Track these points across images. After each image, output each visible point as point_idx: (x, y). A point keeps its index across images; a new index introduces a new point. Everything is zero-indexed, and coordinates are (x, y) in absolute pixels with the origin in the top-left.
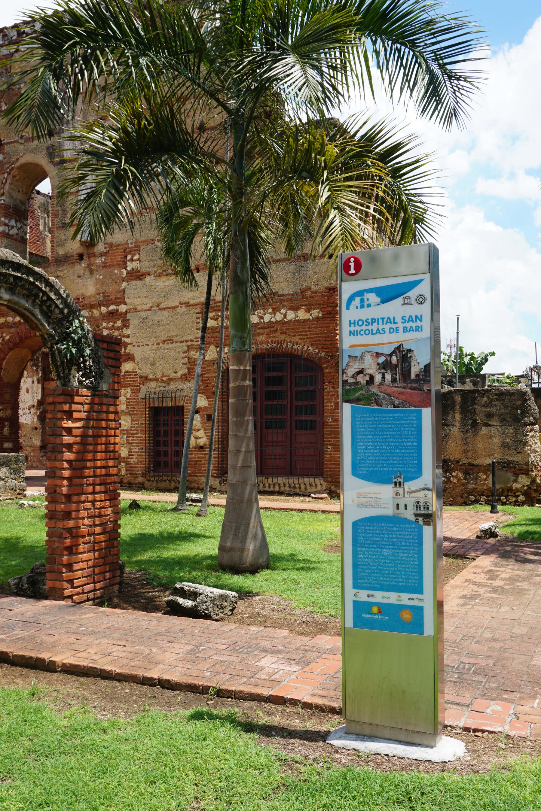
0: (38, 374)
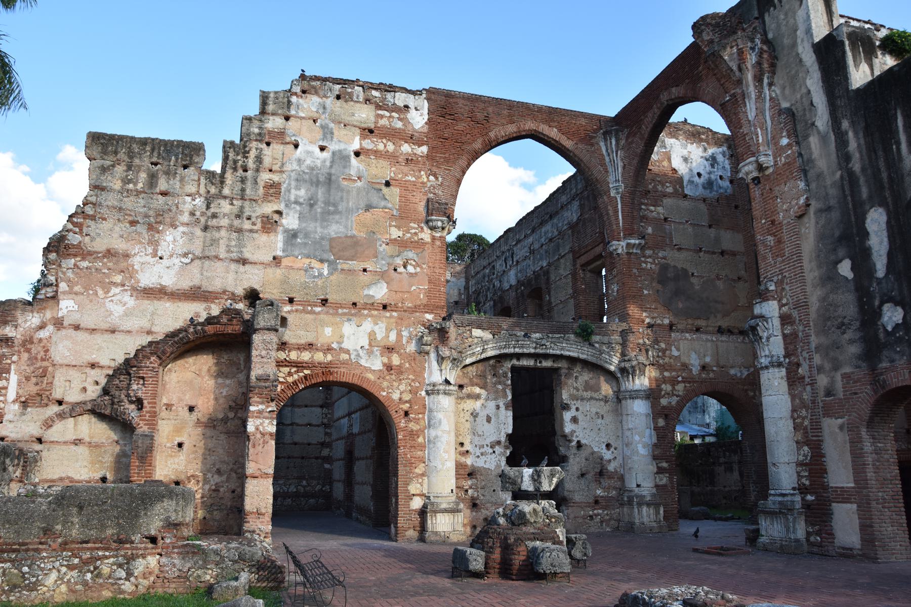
0: (505, 396)
